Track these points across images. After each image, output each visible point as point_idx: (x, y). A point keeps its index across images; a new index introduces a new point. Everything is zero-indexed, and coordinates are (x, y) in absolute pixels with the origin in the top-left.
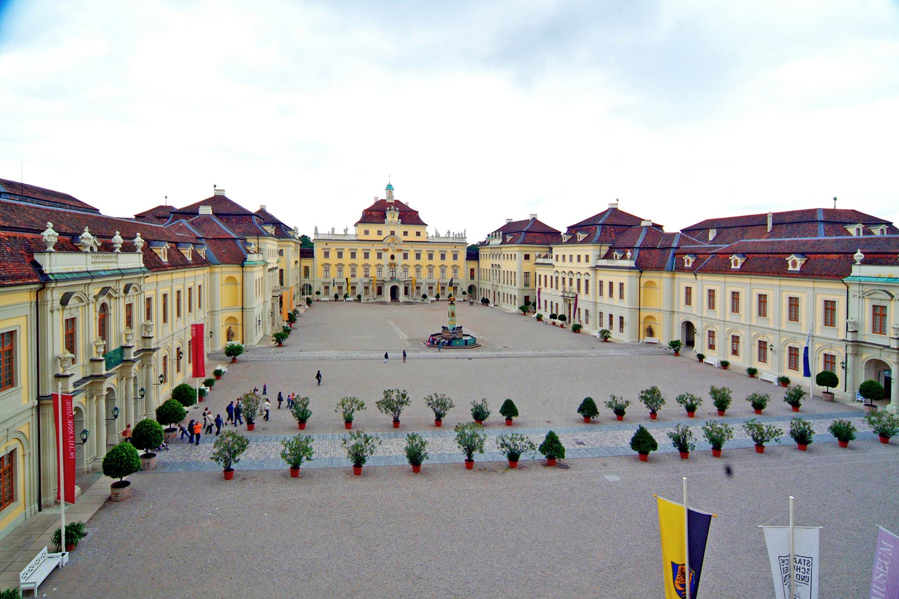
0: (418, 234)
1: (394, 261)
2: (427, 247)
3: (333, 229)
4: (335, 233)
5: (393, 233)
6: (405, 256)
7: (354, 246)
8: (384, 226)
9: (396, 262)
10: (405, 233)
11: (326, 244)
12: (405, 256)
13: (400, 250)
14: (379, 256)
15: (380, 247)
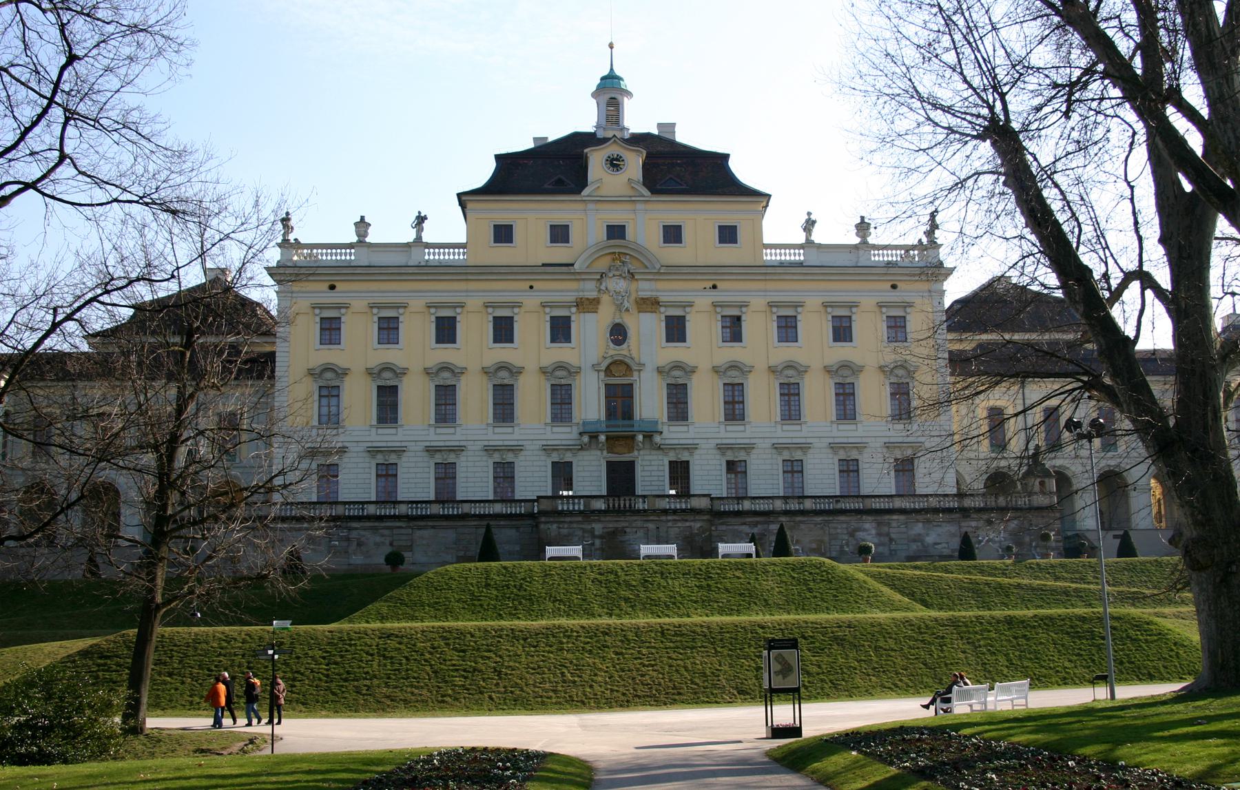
0: (728, 234)
1: (623, 350)
2: (770, 286)
3: (362, 225)
4: (368, 240)
5: (616, 232)
6: (676, 330)
7: (445, 291)
8: (580, 206)
9: (635, 354)
10: (673, 234)
11: (332, 287)
12: (676, 330)
13: (649, 304)
14: (561, 330)
15: (564, 291)
